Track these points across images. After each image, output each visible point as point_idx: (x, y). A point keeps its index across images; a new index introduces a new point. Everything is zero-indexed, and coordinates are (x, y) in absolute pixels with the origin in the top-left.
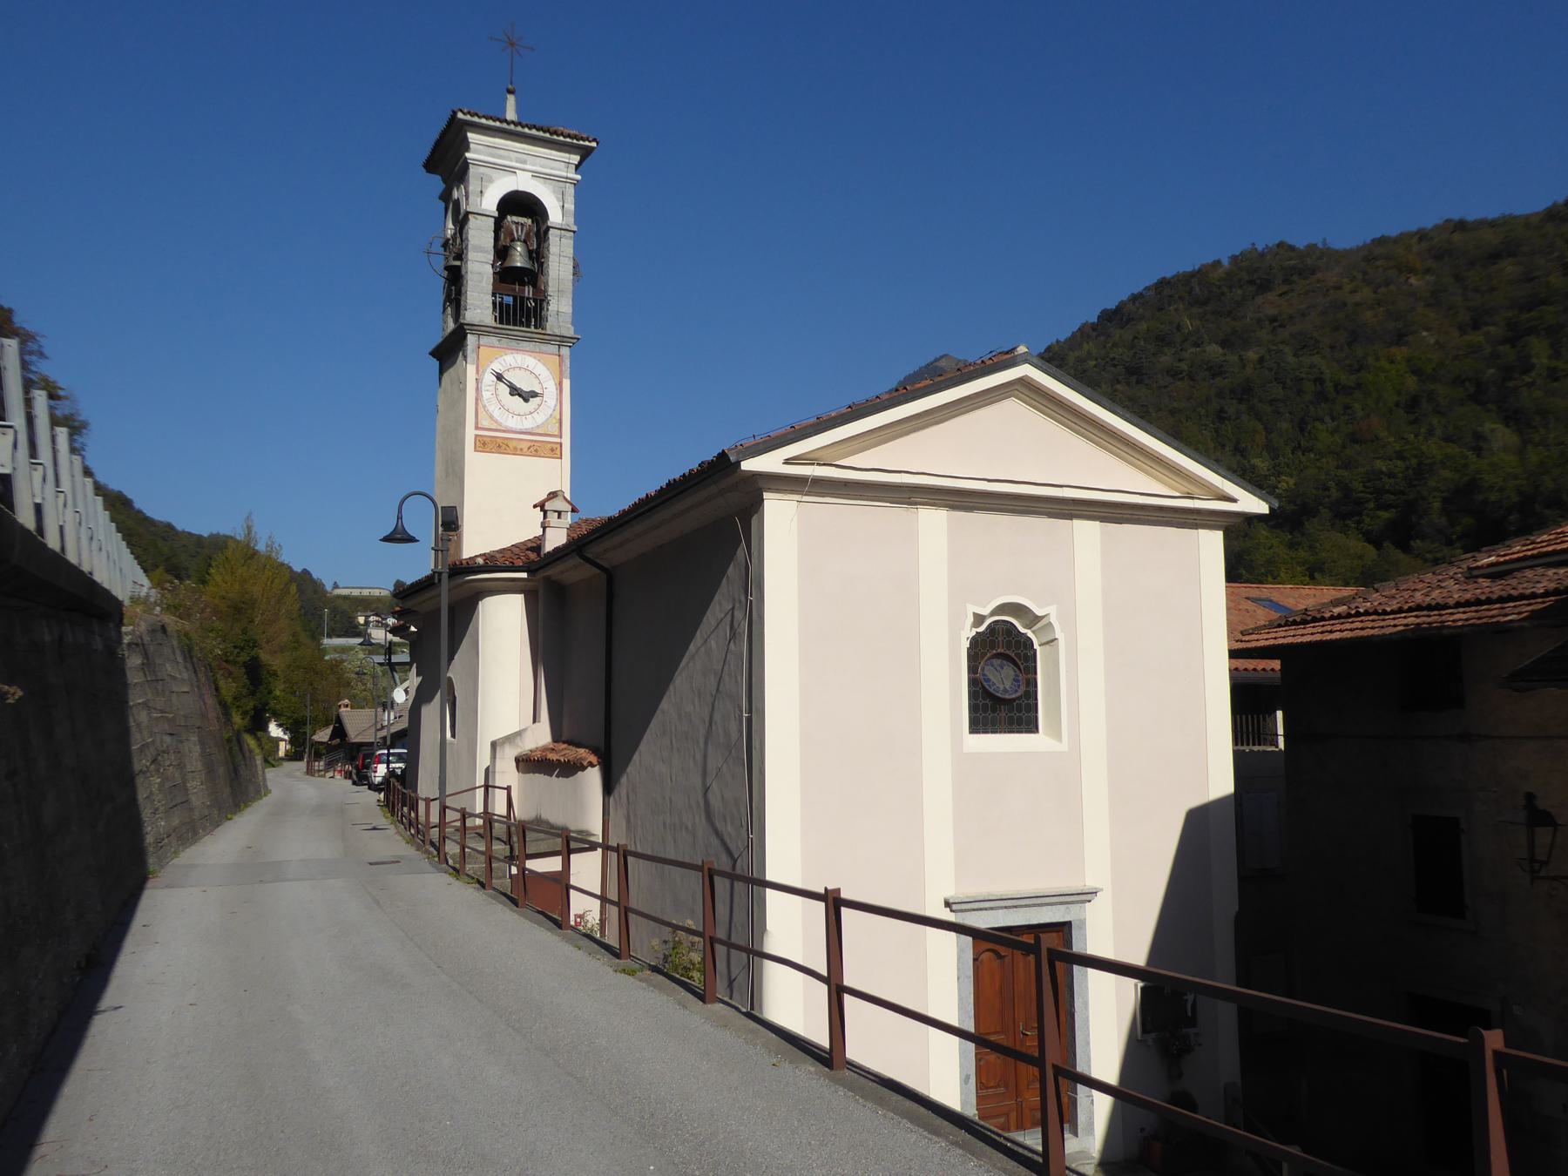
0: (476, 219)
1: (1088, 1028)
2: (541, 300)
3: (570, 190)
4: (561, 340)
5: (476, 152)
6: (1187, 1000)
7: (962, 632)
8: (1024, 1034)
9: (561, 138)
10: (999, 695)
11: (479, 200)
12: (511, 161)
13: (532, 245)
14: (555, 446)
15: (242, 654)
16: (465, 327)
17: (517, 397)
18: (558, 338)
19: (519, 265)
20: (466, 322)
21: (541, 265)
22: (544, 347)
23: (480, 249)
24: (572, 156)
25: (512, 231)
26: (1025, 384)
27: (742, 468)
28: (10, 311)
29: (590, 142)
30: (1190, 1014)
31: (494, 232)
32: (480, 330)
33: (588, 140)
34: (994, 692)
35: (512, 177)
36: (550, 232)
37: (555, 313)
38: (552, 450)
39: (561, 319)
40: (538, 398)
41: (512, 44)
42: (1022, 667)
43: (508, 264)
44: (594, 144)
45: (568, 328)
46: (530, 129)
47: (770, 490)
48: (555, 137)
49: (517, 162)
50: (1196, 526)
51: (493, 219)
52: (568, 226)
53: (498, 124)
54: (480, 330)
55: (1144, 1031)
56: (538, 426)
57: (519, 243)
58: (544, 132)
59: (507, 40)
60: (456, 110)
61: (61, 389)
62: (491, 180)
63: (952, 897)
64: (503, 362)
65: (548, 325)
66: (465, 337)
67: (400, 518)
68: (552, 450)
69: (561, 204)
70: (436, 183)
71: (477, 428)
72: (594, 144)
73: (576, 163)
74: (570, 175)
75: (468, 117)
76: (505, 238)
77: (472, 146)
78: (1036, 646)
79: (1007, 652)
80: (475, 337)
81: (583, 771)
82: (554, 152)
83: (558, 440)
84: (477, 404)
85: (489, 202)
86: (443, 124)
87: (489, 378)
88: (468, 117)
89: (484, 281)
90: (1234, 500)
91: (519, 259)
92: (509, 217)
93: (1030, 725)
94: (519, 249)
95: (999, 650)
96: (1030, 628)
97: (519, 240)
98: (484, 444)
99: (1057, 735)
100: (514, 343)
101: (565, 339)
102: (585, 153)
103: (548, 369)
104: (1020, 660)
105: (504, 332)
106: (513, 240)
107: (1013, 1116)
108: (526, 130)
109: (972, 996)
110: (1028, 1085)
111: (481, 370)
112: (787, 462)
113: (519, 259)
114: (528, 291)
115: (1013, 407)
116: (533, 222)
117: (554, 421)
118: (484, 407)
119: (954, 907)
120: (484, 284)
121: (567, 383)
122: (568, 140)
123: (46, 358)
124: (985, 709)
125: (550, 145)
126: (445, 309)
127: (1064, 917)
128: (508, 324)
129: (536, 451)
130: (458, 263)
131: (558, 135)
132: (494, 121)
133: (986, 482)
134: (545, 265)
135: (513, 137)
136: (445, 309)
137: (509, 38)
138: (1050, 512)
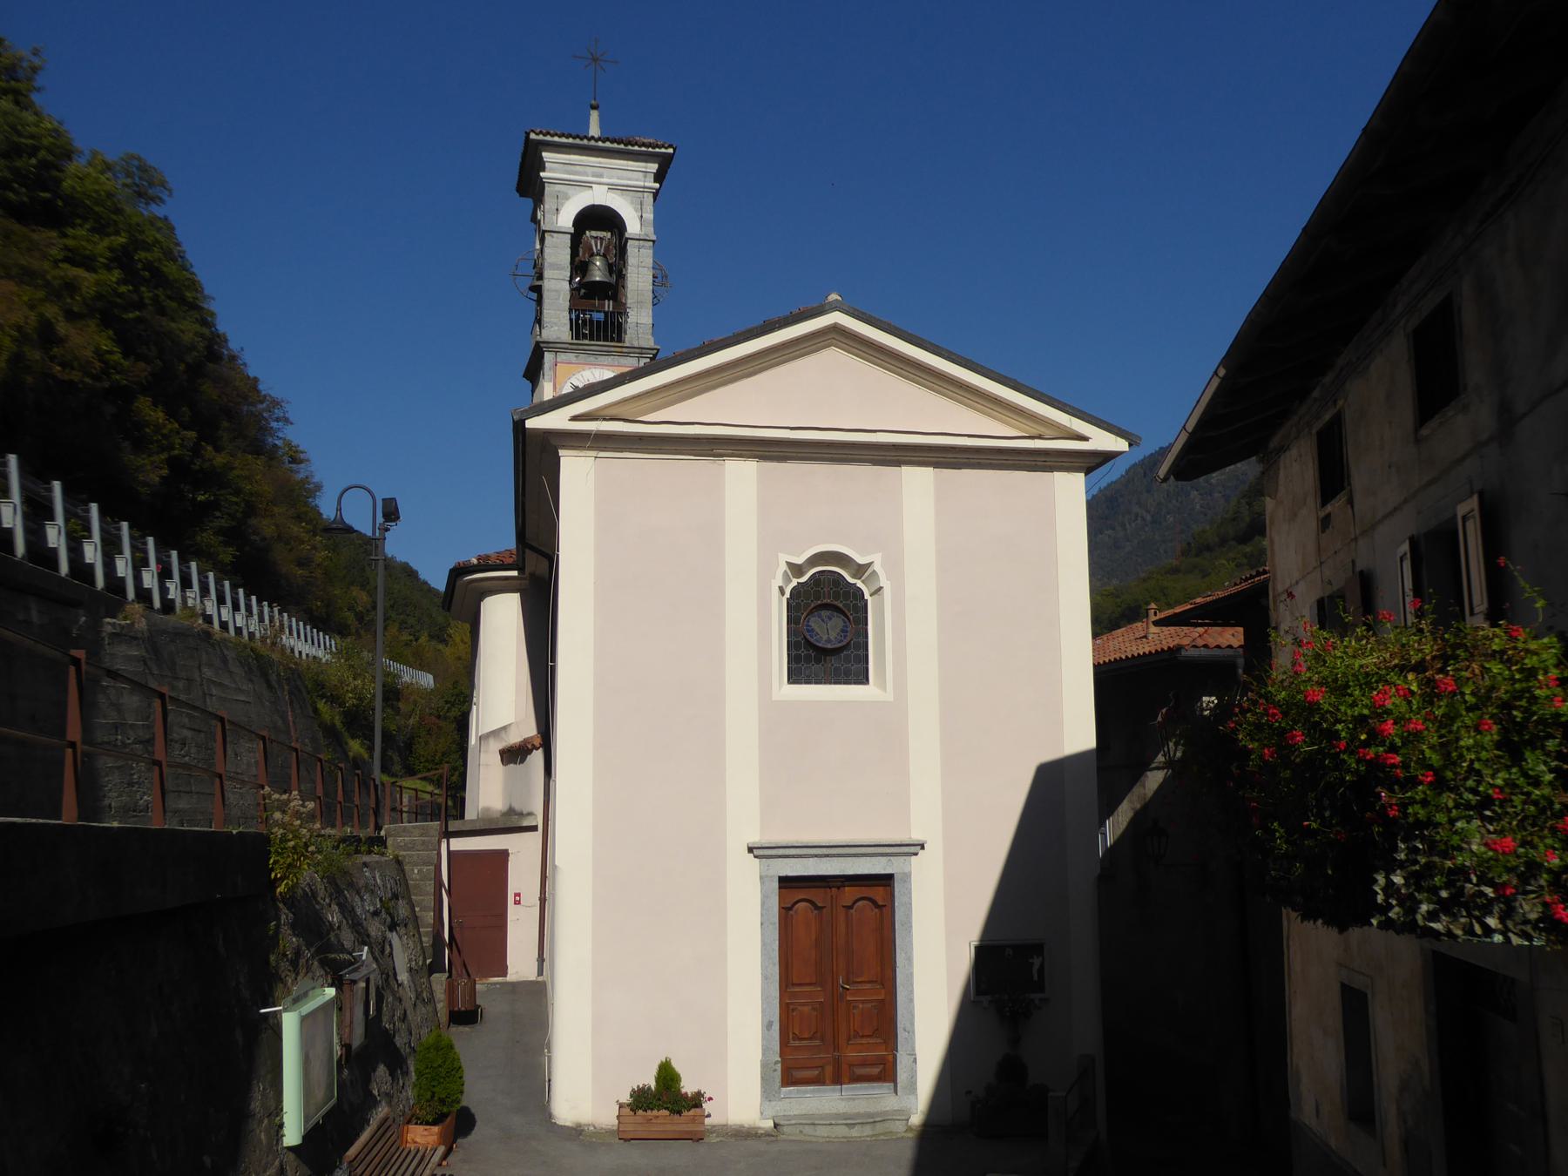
0: (553, 237)
1: (912, 985)
2: (621, 310)
3: (649, 198)
5: (552, 170)
6: (1033, 964)
7: (773, 581)
8: (842, 987)
9: (636, 148)
10: (820, 645)
12: (588, 176)
15: (453, 709)
19: (598, 279)
25: (591, 246)
27: (527, 426)
28: (256, 380)
29: (666, 148)
30: (1036, 977)
31: (571, 248)
32: (557, 347)
33: (663, 146)
34: (815, 643)
35: (589, 192)
36: (628, 244)
41: (595, 60)
42: (851, 617)
43: (587, 279)
44: (671, 151)
46: (604, 142)
47: (564, 447)
48: (630, 147)
49: (593, 176)
50: (1051, 469)
51: (569, 236)
52: (647, 236)
53: (571, 140)
54: (557, 347)
55: (979, 992)
57: (598, 257)
58: (619, 144)
61: (302, 452)
62: (567, 198)
63: (753, 843)
64: (581, 379)
66: (542, 357)
67: (339, 509)
69: (640, 214)
70: (528, 202)
72: (671, 151)
74: (647, 184)
75: (541, 137)
76: (584, 254)
78: (867, 596)
79: (836, 603)
81: (530, 754)
85: (565, 219)
86: (520, 148)
88: (541, 137)
90: (1085, 439)
91: (598, 273)
93: (863, 679)
94: (598, 263)
95: (825, 601)
96: (860, 579)
97: (598, 254)
99: (882, 685)
100: (592, 358)
101: (644, 351)
102: (665, 163)
104: (849, 611)
105: (581, 347)
106: (592, 255)
107: (829, 1069)
108: (600, 144)
109: (777, 942)
110: (849, 1039)
112: (575, 418)
113: (598, 273)
114: (609, 305)
115: (834, 357)
122: (643, 149)
123: (292, 424)
124: (808, 659)
127: (884, 870)
128: (598, 340)
131: (633, 145)
132: (567, 138)
133: (788, 430)
135: (587, 152)
137: (592, 54)
138: (873, 459)
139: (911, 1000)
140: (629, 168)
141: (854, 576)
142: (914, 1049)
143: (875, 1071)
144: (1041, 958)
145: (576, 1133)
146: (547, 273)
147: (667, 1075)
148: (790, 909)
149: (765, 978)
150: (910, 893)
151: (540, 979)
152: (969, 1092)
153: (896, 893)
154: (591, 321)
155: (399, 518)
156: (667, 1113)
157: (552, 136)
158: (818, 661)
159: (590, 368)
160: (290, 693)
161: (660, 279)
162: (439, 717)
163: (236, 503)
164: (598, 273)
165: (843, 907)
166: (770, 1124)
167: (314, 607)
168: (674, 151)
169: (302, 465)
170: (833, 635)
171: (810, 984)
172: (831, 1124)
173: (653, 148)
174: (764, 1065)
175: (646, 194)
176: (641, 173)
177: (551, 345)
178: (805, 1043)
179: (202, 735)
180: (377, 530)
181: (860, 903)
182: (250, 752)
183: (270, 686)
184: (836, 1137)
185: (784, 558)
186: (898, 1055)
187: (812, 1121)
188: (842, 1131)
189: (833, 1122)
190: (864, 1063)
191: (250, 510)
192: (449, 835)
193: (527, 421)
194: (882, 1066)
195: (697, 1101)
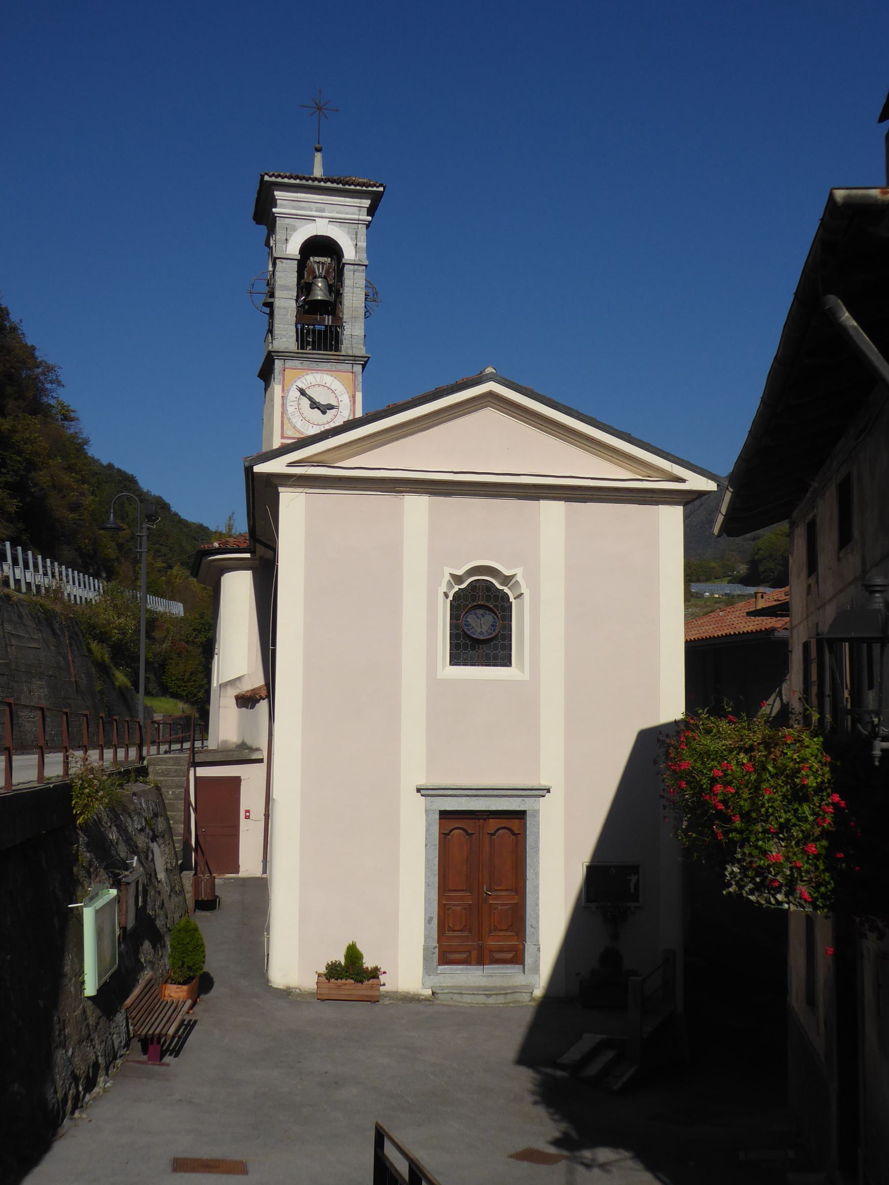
0: (282, 263)
1: (538, 893)
2: (338, 322)
3: (363, 229)
4: (354, 359)
6: (630, 880)
7: (439, 588)
8: (486, 893)
9: (352, 187)
10: (473, 636)
11: (284, 246)
12: (312, 211)
15: (200, 636)
16: (273, 354)
17: (316, 409)
19: (319, 298)
22: (340, 366)
23: (285, 288)
25: (314, 269)
26: (491, 394)
27: (254, 471)
28: (33, 348)
29: (377, 187)
30: (632, 890)
31: (297, 272)
32: (285, 355)
33: (374, 186)
36: (345, 268)
37: (350, 336)
39: (354, 341)
41: (320, 109)
43: (310, 298)
44: (381, 189)
45: (361, 349)
48: (347, 187)
49: (316, 211)
50: (657, 503)
51: (296, 262)
52: (361, 261)
53: (298, 181)
54: (285, 355)
57: (320, 280)
58: (338, 183)
59: (315, 106)
60: (263, 174)
62: (294, 229)
64: (305, 382)
69: (355, 243)
71: (283, 437)
72: (381, 189)
73: (368, 206)
74: (361, 217)
75: (273, 179)
76: (308, 276)
77: (278, 202)
78: (512, 599)
80: (281, 362)
81: (258, 703)
84: (282, 417)
85: (293, 248)
87: (294, 394)
88: (273, 179)
89: (289, 313)
90: (682, 480)
91: (320, 293)
92: (311, 258)
93: (506, 661)
94: (320, 285)
95: (479, 603)
96: (506, 586)
97: (320, 277)
99: (521, 668)
100: (314, 364)
101: (357, 358)
102: (376, 200)
103: (343, 385)
104: (498, 611)
105: (305, 356)
106: (315, 277)
107: (474, 953)
108: (322, 184)
109: (437, 859)
110: (490, 932)
111: (286, 388)
113: (320, 293)
114: (328, 320)
115: (490, 415)
118: (289, 419)
119: (423, 792)
120: (289, 317)
121: (359, 396)
122: (358, 188)
123: (63, 386)
124: (466, 647)
127: (519, 807)
131: (350, 185)
132: (295, 179)
139: (537, 905)
140: (346, 204)
141: (502, 584)
142: (538, 940)
143: (510, 956)
144: (636, 877)
145: (286, 993)
146: (278, 293)
147: (353, 955)
148: (448, 834)
149: (428, 885)
150: (539, 825)
151: (264, 876)
152: (578, 974)
153: (528, 825)
154: (314, 330)
156: (353, 981)
157: (283, 178)
158: (473, 648)
159: (312, 373)
160: (70, 638)
161: (371, 297)
162: (188, 642)
163: (19, 462)
164: (319, 292)
165: (488, 833)
166: (429, 992)
167: (83, 546)
168: (384, 188)
169: (73, 423)
170: (485, 628)
171: (462, 890)
172: (474, 994)
173: (367, 187)
174: (426, 949)
175: (360, 225)
176: (356, 208)
177: (280, 354)
178: (457, 934)
179: (5, 677)
181: (501, 831)
182: (41, 688)
183: (54, 634)
184: (477, 1004)
185: (448, 571)
186: (526, 945)
187: (460, 991)
188: (482, 999)
189: (475, 992)
190: (501, 950)
191: (31, 466)
192: (195, 765)
193: (254, 467)
194: (514, 953)
195: (375, 974)
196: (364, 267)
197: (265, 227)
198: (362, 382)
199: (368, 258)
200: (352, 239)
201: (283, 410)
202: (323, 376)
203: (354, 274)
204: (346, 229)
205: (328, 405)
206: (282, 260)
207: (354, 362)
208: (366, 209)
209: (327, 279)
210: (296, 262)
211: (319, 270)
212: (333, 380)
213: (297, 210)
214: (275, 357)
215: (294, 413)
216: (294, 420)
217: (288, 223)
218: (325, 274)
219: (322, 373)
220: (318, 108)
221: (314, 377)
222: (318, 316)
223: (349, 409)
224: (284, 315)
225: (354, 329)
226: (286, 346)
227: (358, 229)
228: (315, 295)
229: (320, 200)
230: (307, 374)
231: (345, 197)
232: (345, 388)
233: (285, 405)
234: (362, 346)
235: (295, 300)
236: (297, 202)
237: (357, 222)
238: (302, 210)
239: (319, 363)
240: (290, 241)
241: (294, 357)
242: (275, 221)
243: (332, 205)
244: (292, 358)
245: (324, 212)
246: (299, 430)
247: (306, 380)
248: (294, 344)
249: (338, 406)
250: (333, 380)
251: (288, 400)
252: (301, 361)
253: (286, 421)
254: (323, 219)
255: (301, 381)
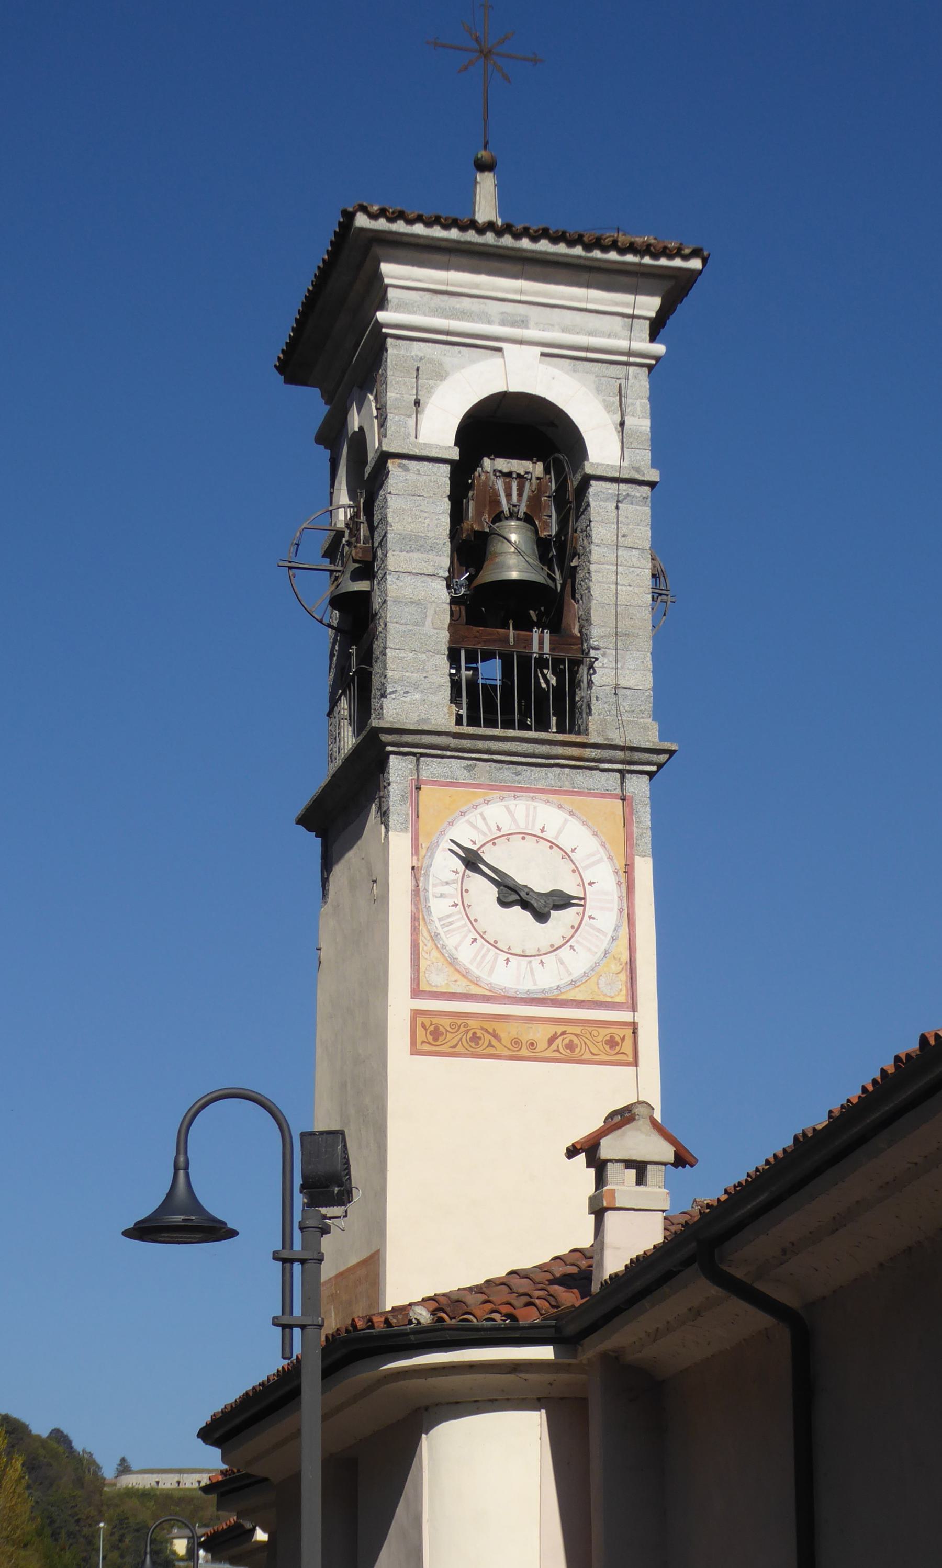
0: (406, 469)
5: (399, 308)
9: (613, 255)
11: (412, 422)
12: (490, 322)
13: (547, 525)
14: (619, 1032)
16: (385, 738)
17: (517, 908)
18: (620, 754)
19: (514, 575)
20: (383, 724)
21: (571, 574)
22: (583, 779)
23: (416, 543)
24: (641, 299)
25: (496, 494)
29: (686, 258)
33: (678, 253)
36: (592, 490)
37: (610, 690)
38: (612, 1043)
39: (625, 705)
40: (572, 911)
41: (486, 54)
43: (488, 575)
44: (695, 264)
45: (645, 728)
48: (597, 254)
49: (503, 323)
52: (637, 470)
53: (454, 234)
56: (573, 983)
59: (475, 45)
60: (350, 209)
62: (441, 375)
64: (480, 823)
65: (593, 722)
66: (381, 765)
68: (612, 1043)
69: (618, 418)
71: (417, 992)
72: (695, 264)
73: (653, 314)
75: (382, 224)
76: (479, 514)
77: (392, 293)
82: (594, 293)
83: (626, 1016)
84: (415, 931)
86: (319, 253)
88: (382, 224)
89: (429, 621)
92: (487, 462)
94: (514, 537)
97: (513, 516)
98: (436, 1034)
100: (507, 773)
101: (637, 756)
103: (595, 834)
105: (480, 744)
106: (498, 517)
111: (424, 843)
116: (547, 471)
117: (615, 967)
118: (435, 937)
120: (428, 628)
121: (644, 869)
122: (630, 258)
125: (585, 276)
126: (334, 703)
128: (491, 724)
129: (571, 1046)
130: (363, 586)
131: (605, 249)
132: (446, 227)
134: (581, 574)
136: (334, 703)
137: (477, 40)
140: (591, 306)
155: (350, 1192)
157: (410, 222)
159: (502, 799)
168: (705, 262)
173: (655, 256)
176: (618, 319)
180: (297, 1235)
196: (647, 489)
197: (317, 391)
198: (653, 828)
199: (655, 463)
200: (608, 407)
201: (417, 909)
202: (535, 808)
203: (617, 508)
204: (592, 378)
205: (554, 893)
206: (404, 462)
207: (628, 767)
208: (647, 323)
209: (534, 524)
210: (446, 469)
211: (509, 495)
212: (566, 821)
213: (447, 317)
214: (389, 748)
215: (450, 920)
216: (450, 941)
217: (420, 354)
218: (528, 506)
219: (532, 799)
220: (481, 52)
221: (507, 808)
222: (512, 632)
223: (616, 911)
224: (416, 624)
225: (622, 667)
226: (423, 716)
227: (627, 379)
228: (504, 567)
229: (515, 291)
230: (487, 802)
231: (588, 286)
232: (603, 845)
233: (422, 893)
234: (650, 720)
235: (446, 579)
236: (445, 297)
237: (624, 359)
238: (459, 319)
239: (520, 768)
240: (429, 405)
241: (447, 748)
242: (383, 348)
243: (548, 309)
244: (441, 752)
245: (527, 327)
246: (468, 971)
247: (484, 819)
248: (446, 710)
249: (584, 899)
250: (566, 821)
251: (431, 879)
252: (470, 762)
253: (426, 945)
254: (524, 347)
255: (469, 822)
